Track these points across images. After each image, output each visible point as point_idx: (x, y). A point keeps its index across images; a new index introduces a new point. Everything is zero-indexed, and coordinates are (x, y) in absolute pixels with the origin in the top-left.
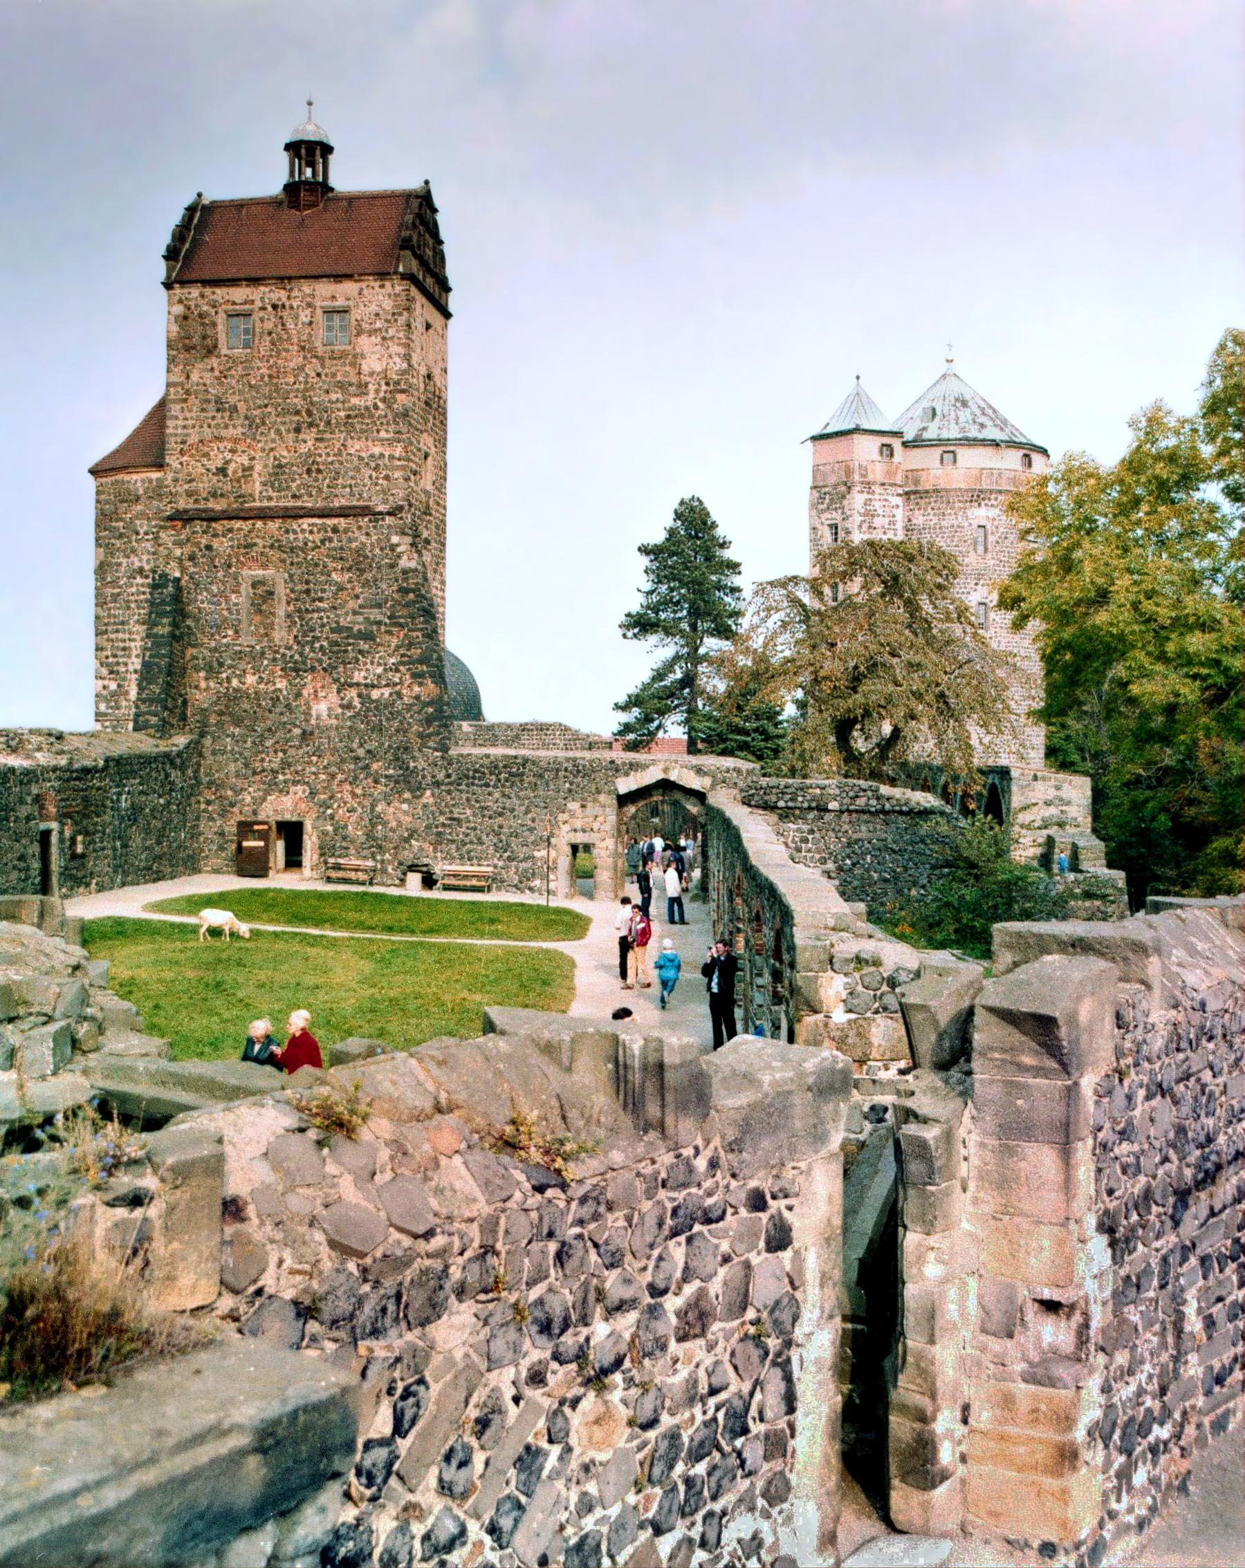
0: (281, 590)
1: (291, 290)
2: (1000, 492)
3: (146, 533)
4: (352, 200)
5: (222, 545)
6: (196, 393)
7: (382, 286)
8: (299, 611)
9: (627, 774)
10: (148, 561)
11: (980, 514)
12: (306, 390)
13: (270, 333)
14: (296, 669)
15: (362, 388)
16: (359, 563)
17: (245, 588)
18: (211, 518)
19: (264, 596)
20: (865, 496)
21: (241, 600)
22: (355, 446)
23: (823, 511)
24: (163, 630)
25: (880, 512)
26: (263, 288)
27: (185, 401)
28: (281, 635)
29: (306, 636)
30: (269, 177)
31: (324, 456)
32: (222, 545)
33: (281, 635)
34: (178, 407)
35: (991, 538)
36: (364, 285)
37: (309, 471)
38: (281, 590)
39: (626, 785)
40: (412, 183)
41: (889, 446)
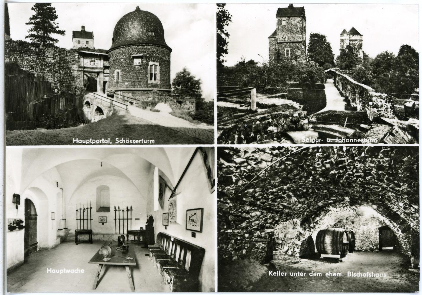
0: (289, 51)
5: (283, 46)
14: (291, 59)
15: (297, 28)
16: (298, 47)
17: (286, 51)
18: (281, 43)
19: (288, 51)
21: (285, 52)
22: (297, 35)
28: (289, 55)
29: (292, 56)
31: (294, 36)
32: (283, 46)
33: (289, 55)
38: (289, 51)
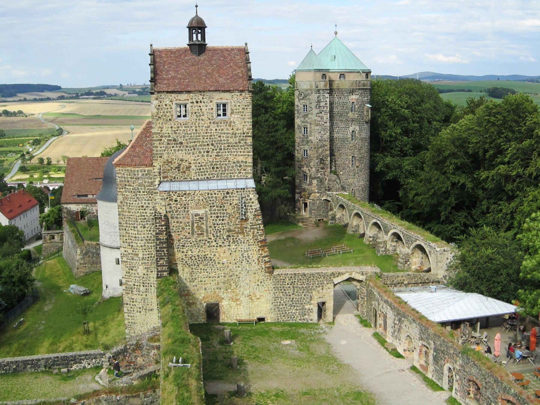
1: (204, 95)
2: (359, 89)
3: (143, 192)
4: (215, 50)
6: (166, 137)
7: (241, 95)
8: (214, 224)
9: (338, 276)
10: (145, 203)
11: (354, 97)
12: (211, 136)
13: (196, 113)
20: (318, 95)
23: (301, 99)
24: (163, 237)
25: (322, 100)
26: (192, 94)
27: (161, 140)
30: (181, 40)
34: (158, 142)
35: (356, 107)
36: (233, 94)
37: (213, 168)
39: (336, 280)
40: (241, 45)
41: (324, 75)
